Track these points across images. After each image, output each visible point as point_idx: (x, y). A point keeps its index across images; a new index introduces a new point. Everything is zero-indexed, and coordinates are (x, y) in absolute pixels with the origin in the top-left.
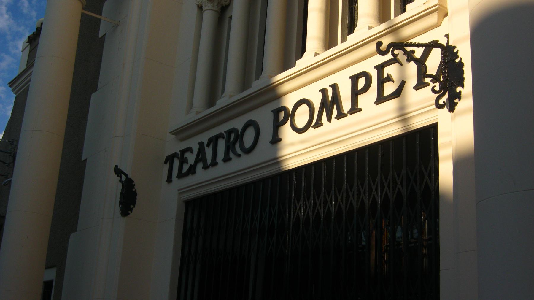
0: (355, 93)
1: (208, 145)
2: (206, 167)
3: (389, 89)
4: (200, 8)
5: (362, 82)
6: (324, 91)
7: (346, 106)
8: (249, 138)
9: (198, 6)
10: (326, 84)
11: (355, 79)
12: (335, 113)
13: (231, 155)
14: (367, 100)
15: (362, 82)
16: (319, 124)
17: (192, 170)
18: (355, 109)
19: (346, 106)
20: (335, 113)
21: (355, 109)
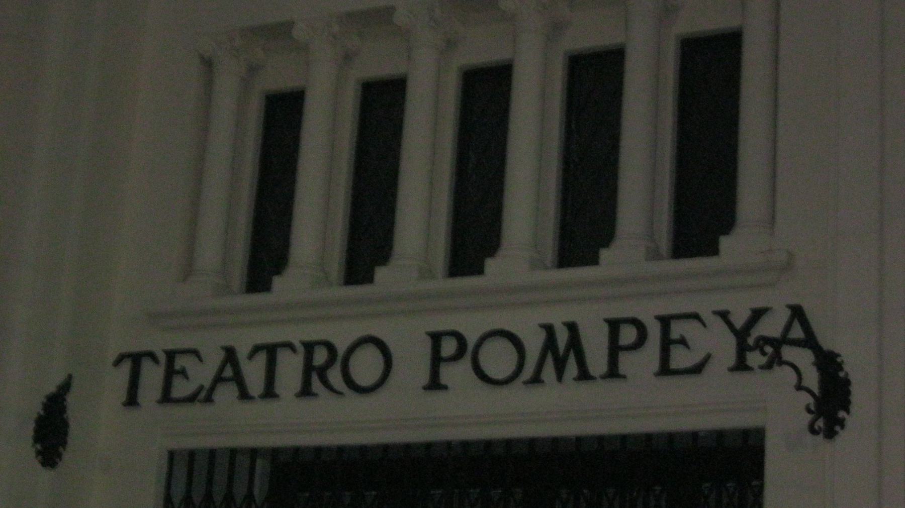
0: (615, 349)
2: (244, 395)
3: (680, 358)
4: (208, 64)
5: (628, 335)
6: (549, 329)
7: (597, 362)
8: (366, 366)
9: (202, 58)
10: (557, 317)
11: (614, 325)
12: (572, 369)
14: (641, 364)
16: (536, 379)
17: (204, 397)
18: (613, 372)
19: (597, 362)
20: (572, 369)
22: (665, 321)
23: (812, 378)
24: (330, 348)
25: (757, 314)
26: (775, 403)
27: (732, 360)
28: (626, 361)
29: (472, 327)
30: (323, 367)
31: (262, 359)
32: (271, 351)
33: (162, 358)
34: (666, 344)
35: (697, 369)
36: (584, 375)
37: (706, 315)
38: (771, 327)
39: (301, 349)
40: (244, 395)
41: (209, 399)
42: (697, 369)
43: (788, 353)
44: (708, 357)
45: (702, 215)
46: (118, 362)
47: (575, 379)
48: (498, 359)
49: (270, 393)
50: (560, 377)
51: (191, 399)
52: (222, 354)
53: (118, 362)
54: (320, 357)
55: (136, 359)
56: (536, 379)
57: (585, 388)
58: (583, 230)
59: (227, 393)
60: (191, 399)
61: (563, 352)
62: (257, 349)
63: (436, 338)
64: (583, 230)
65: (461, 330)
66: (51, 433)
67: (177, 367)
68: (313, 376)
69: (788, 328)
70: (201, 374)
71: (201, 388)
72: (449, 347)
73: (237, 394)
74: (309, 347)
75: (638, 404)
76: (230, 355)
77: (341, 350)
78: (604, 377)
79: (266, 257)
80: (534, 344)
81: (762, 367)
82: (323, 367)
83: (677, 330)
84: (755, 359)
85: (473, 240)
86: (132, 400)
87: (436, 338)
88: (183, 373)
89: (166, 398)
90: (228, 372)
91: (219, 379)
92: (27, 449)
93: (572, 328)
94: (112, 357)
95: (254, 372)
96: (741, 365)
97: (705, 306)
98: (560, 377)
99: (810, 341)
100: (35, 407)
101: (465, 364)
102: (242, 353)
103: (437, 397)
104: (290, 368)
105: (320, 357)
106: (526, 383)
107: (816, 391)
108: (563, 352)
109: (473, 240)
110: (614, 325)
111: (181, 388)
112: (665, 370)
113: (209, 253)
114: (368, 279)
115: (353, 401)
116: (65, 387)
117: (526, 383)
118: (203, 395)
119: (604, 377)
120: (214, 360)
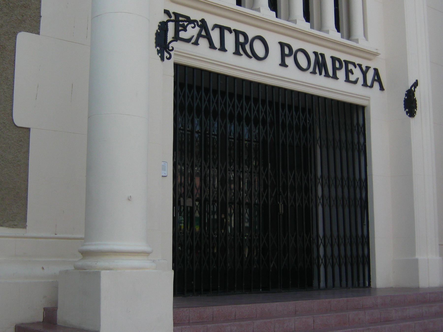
2: (212, 46)
18: (335, 77)
21: (335, 77)
31: (217, 31)
32: (222, 29)
36: (327, 75)
40: (212, 46)
42: (355, 82)
49: (223, 49)
50: (320, 74)
56: (314, 72)
62: (216, 26)
83: (351, 67)
91: (199, 35)
98: (320, 74)
101: (292, 57)
102: (210, 26)
112: (347, 80)
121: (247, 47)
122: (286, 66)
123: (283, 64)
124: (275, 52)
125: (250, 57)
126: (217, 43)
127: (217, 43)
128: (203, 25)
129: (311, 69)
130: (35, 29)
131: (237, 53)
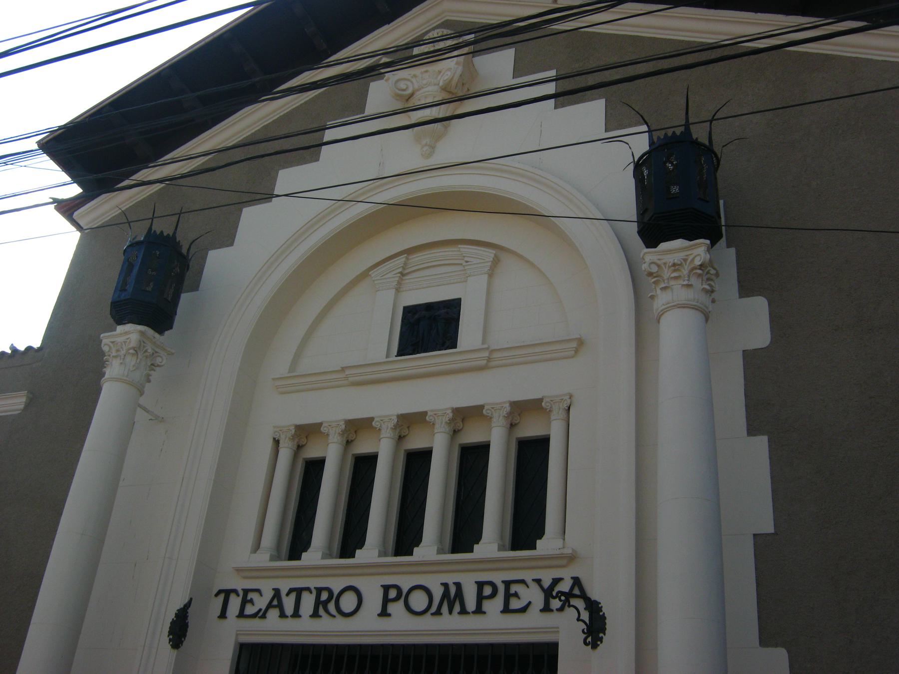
0: (480, 598)
1: (287, 595)
2: (283, 615)
3: (515, 604)
4: (277, 442)
5: (487, 591)
6: (446, 585)
7: (471, 605)
8: (348, 602)
9: (274, 439)
10: (450, 579)
11: (480, 585)
12: (457, 608)
13: (321, 611)
14: (494, 606)
15: (487, 591)
16: (438, 613)
17: (261, 615)
18: (479, 610)
19: (471, 605)
20: (457, 608)
21: (479, 610)
22: (507, 584)
23: (585, 616)
24: (330, 591)
25: (556, 581)
26: (566, 629)
27: (541, 606)
28: (487, 605)
29: (406, 583)
30: (326, 601)
31: (293, 596)
32: (299, 592)
33: (241, 593)
34: (508, 596)
35: (524, 610)
36: (463, 611)
37: (529, 581)
38: (564, 587)
39: (314, 592)
41: (264, 616)
42: (524, 610)
43: (573, 601)
44: (530, 603)
45: (526, 527)
46: (217, 595)
47: (459, 613)
48: (419, 601)
49: (296, 614)
50: (450, 612)
51: (254, 616)
52: (272, 593)
53: (217, 595)
54: (324, 596)
55: (227, 593)
56: (438, 613)
57: (464, 618)
58: (464, 533)
59: (274, 613)
60: (254, 616)
61: (452, 598)
62: (291, 591)
63: (386, 588)
64: (464, 533)
65: (398, 584)
66: (179, 631)
67: (249, 598)
68: (320, 606)
69: (572, 588)
70: (261, 602)
71: (260, 610)
72: (393, 594)
73: (278, 614)
74: (319, 590)
75: (492, 626)
76: (277, 592)
77: (336, 592)
78: (474, 612)
79: (298, 542)
80: (438, 593)
81: (558, 610)
82: (326, 601)
83: (514, 588)
84: (556, 604)
85: (406, 538)
86: (223, 615)
87: (386, 588)
88: (251, 601)
89: (241, 615)
90: (275, 603)
91: (270, 606)
92: (165, 639)
93: (458, 585)
94: (215, 591)
95: (289, 604)
96: (546, 609)
97: (528, 576)
98: (450, 612)
99: (584, 596)
100: (171, 616)
103: (385, 620)
104: (308, 602)
105: (324, 596)
106: (432, 614)
107: (588, 622)
108: (452, 598)
109: (406, 538)
110: (480, 585)
111: (250, 610)
112: (506, 610)
113: (269, 538)
114: (352, 556)
115: (340, 620)
116: (188, 605)
117: (432, 614)
118: (261, 614)
119: (474, 612)
120: (268, 595)
121: (331, 606)
122: (389, 615)
123: (384, 613)
124: (373, 600)
125: (334, 616)
126: (289, 610)
127: (289, 610)
128: (277, 592)
129: (434, 609)
130: (749, 357)
131: (315, 615)
